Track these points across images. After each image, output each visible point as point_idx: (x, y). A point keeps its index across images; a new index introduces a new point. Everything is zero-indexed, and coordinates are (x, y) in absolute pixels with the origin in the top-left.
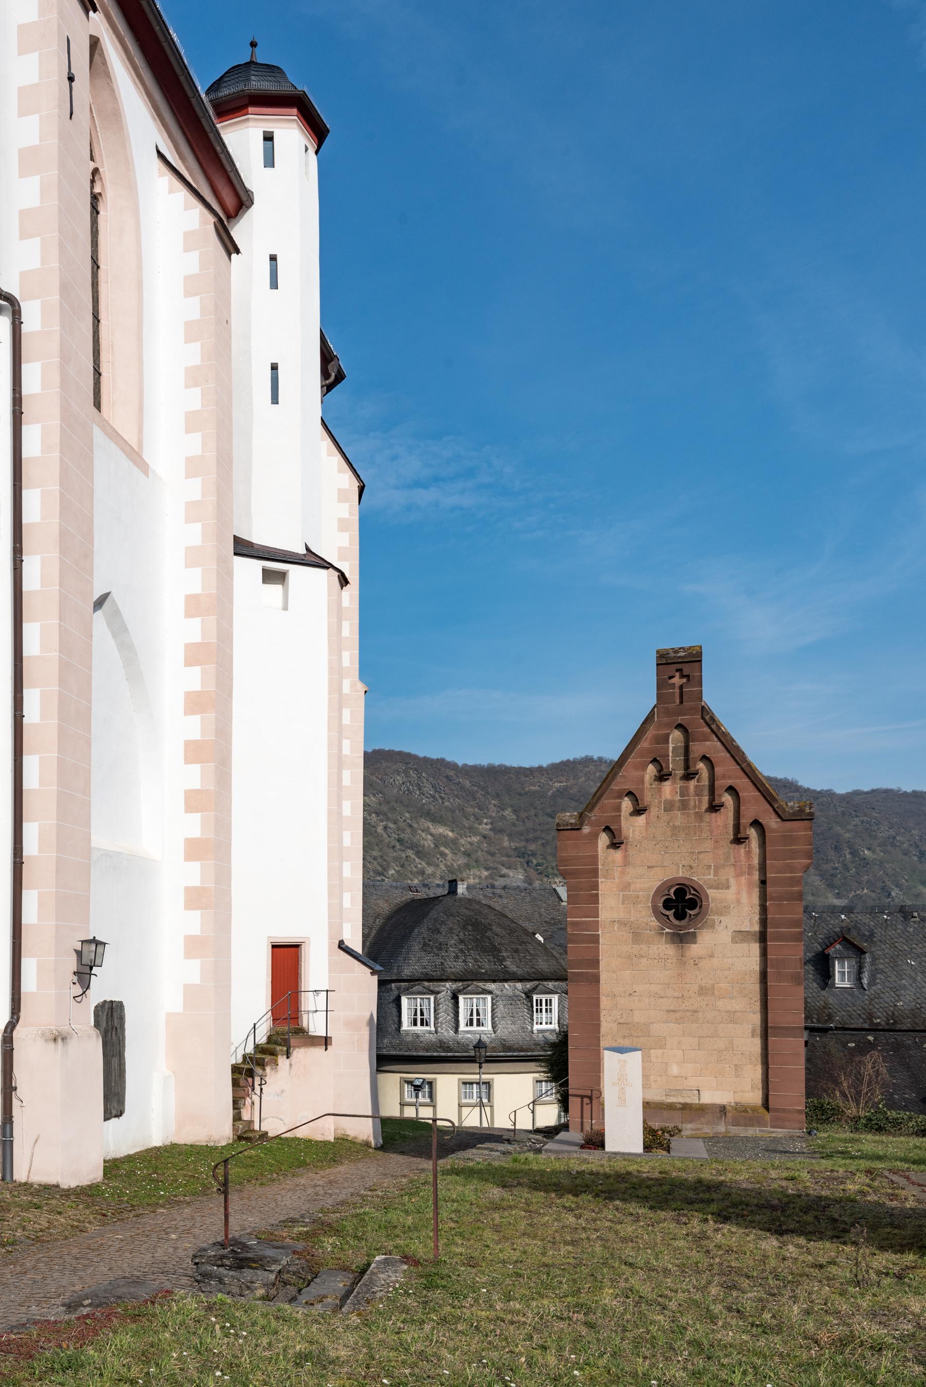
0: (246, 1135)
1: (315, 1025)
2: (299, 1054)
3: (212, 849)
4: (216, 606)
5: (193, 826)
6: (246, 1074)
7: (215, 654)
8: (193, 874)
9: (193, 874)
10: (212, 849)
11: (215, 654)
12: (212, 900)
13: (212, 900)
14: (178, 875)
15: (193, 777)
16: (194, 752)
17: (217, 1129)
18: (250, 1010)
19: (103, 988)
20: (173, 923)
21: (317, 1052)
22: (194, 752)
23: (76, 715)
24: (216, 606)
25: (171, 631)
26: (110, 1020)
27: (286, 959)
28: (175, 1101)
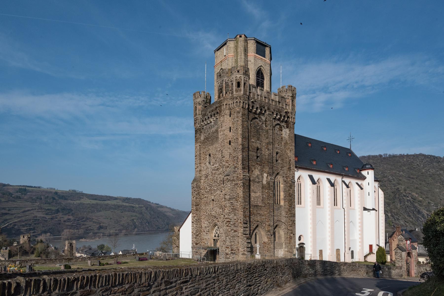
0: (366, 261)
1: (373, 252)
2: (372, 255)
3: (362, 238)
4: (362, 216)
5: (360, 236)
6: (365, 257)
7: (362, 218)
8: (360, 240)
9: (360, 240)
10: (362, 238)
11: (362, 218)
12: (362, 242)
13: (362, 242)
14: (358, 240)
15: (360, 232)
16: (359, 230)
17: (362, 260)
18: (367, 251)
19: (351, 250)
20: (358, 244)
21: (373, 255)
22: (359, 230)
23: (349, 233)
24: (362, 216)
25: (358, 217)
26: (352, 252)
27: (371, 246)
28: (358, 258)
